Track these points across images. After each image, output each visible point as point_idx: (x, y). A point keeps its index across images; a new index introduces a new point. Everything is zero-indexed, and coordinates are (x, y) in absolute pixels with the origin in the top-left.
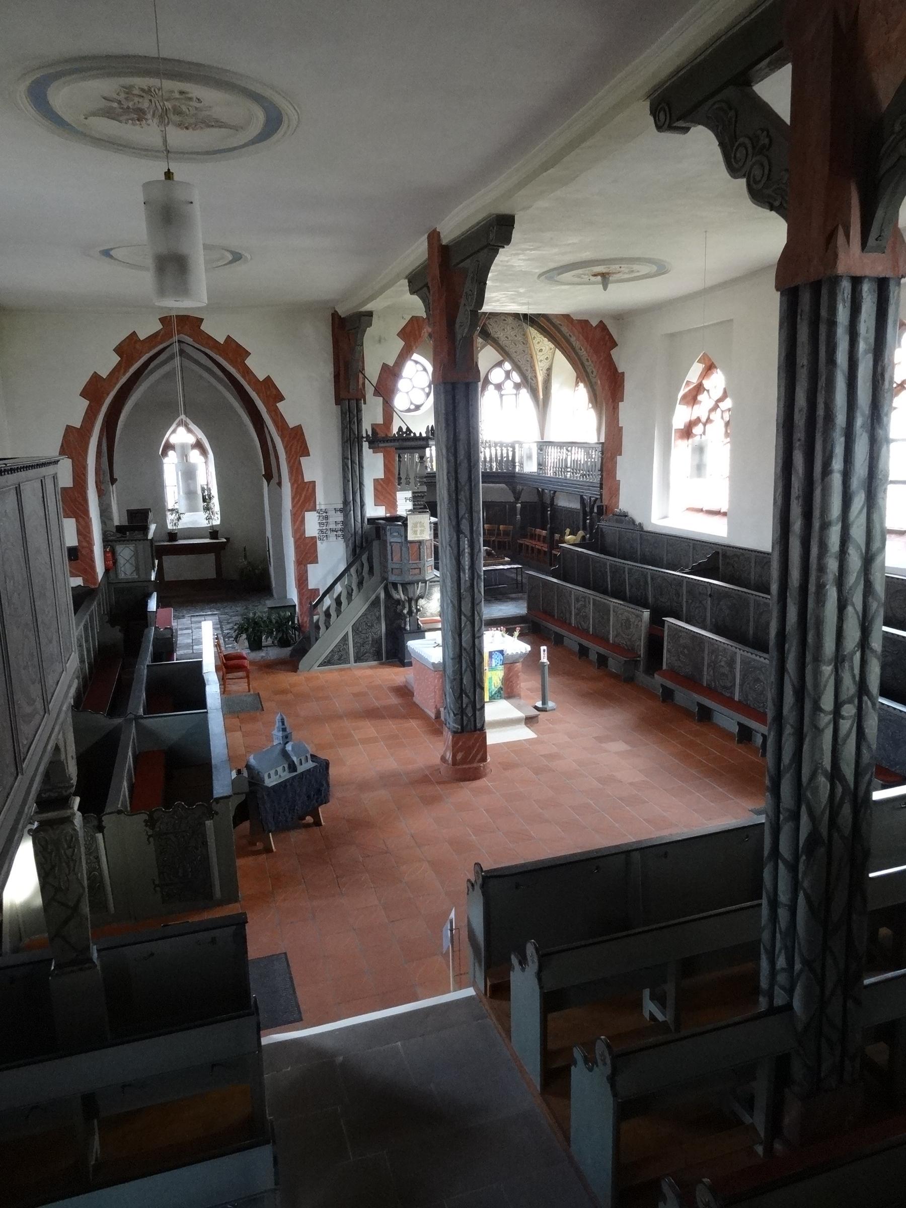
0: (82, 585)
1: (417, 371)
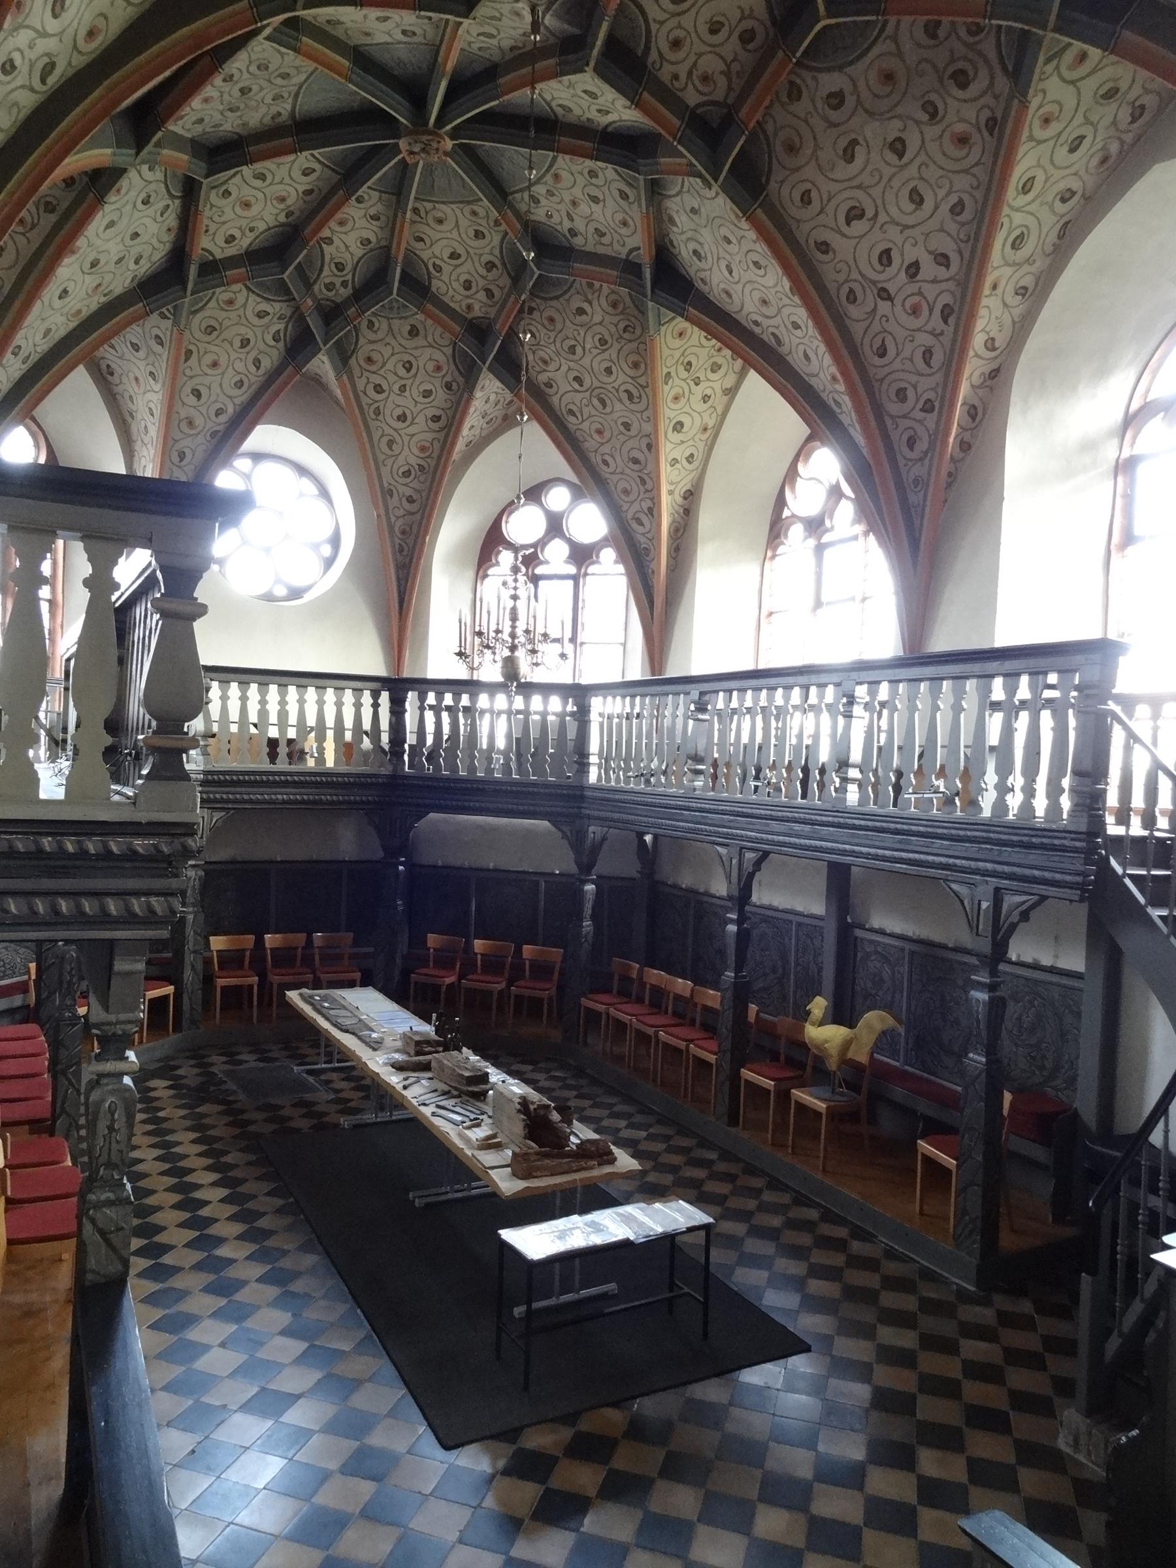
1: (301, 495)
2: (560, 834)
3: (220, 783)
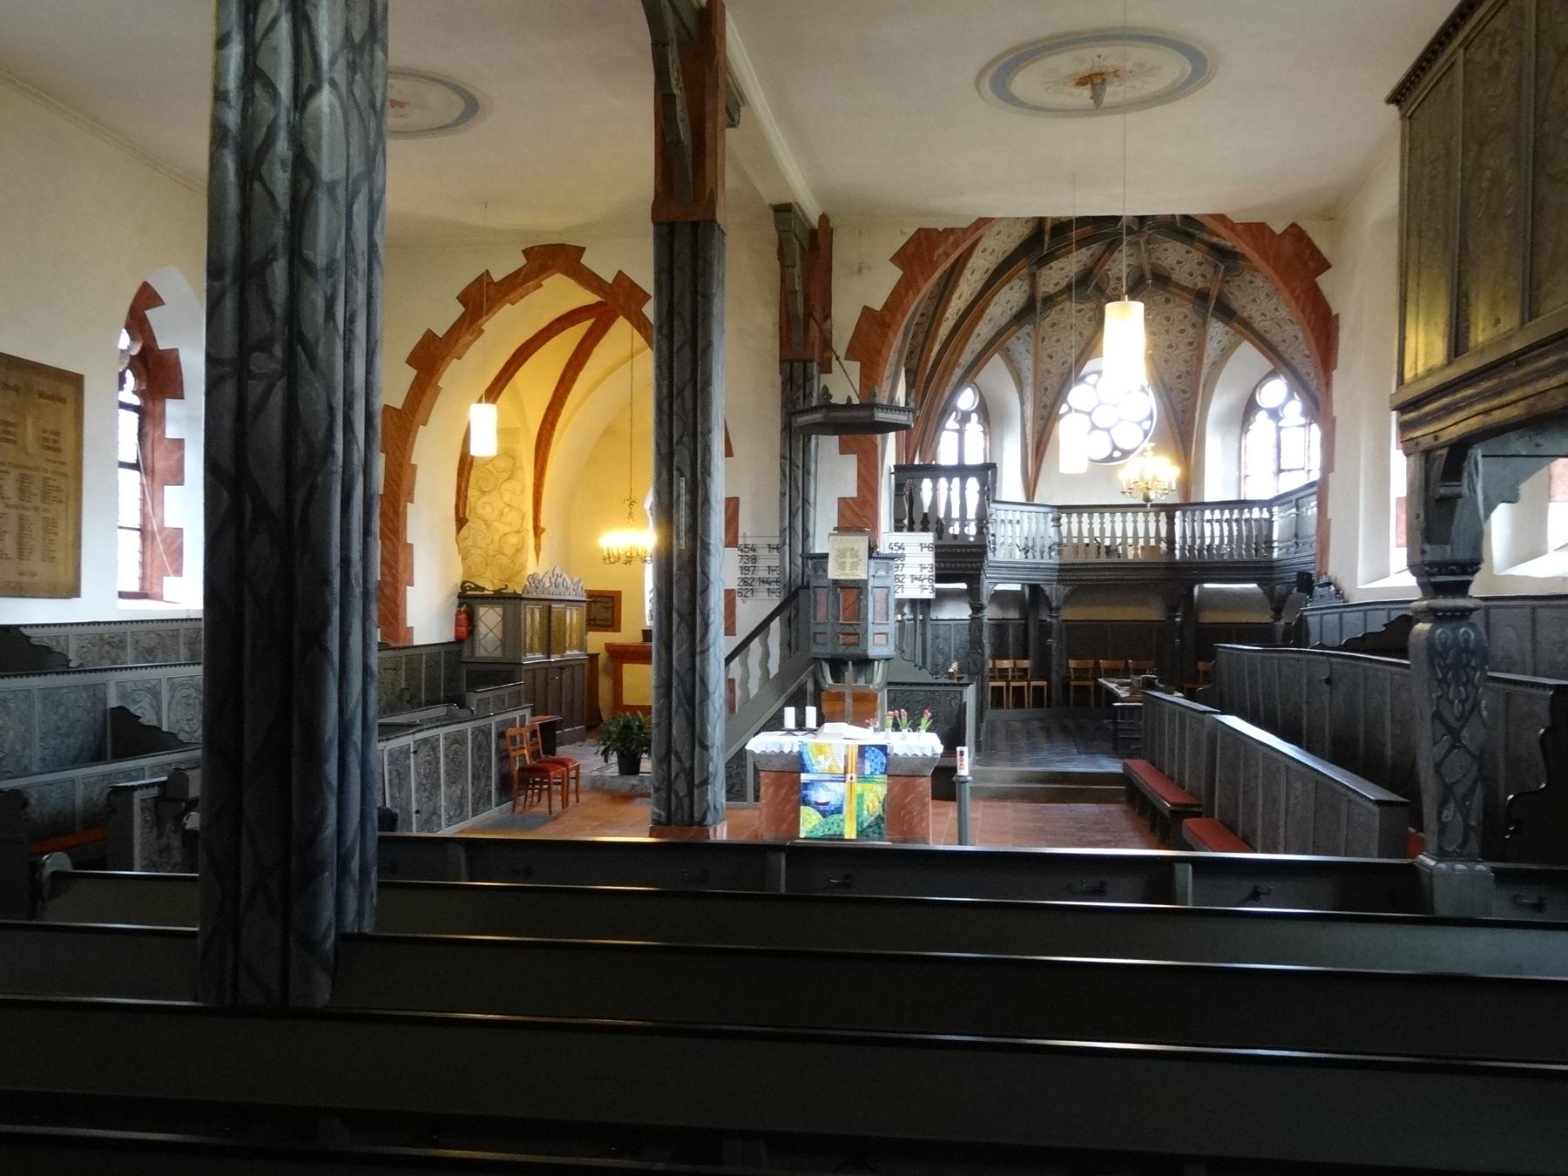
2: (1260, 591)
3: (1068, 570)
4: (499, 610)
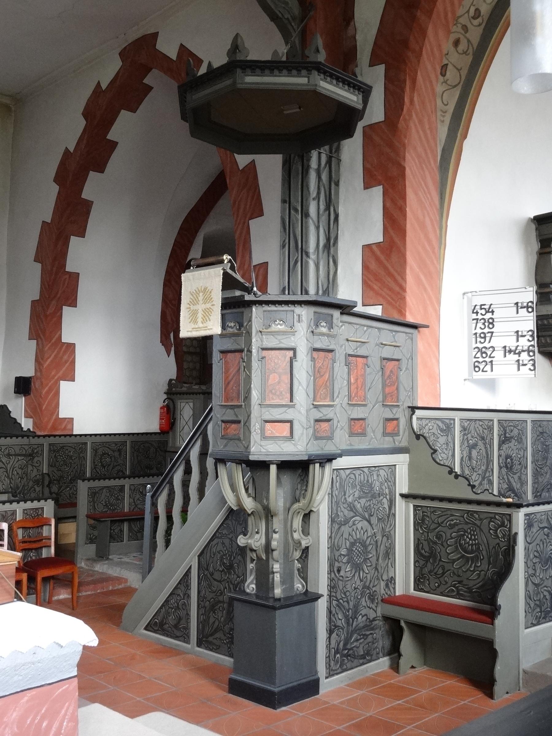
0: (32, 430)
4: (191, 404)
